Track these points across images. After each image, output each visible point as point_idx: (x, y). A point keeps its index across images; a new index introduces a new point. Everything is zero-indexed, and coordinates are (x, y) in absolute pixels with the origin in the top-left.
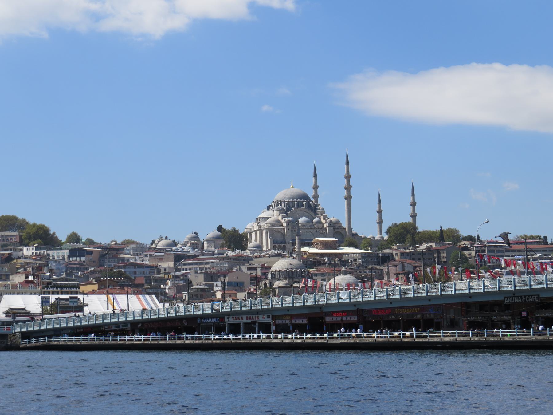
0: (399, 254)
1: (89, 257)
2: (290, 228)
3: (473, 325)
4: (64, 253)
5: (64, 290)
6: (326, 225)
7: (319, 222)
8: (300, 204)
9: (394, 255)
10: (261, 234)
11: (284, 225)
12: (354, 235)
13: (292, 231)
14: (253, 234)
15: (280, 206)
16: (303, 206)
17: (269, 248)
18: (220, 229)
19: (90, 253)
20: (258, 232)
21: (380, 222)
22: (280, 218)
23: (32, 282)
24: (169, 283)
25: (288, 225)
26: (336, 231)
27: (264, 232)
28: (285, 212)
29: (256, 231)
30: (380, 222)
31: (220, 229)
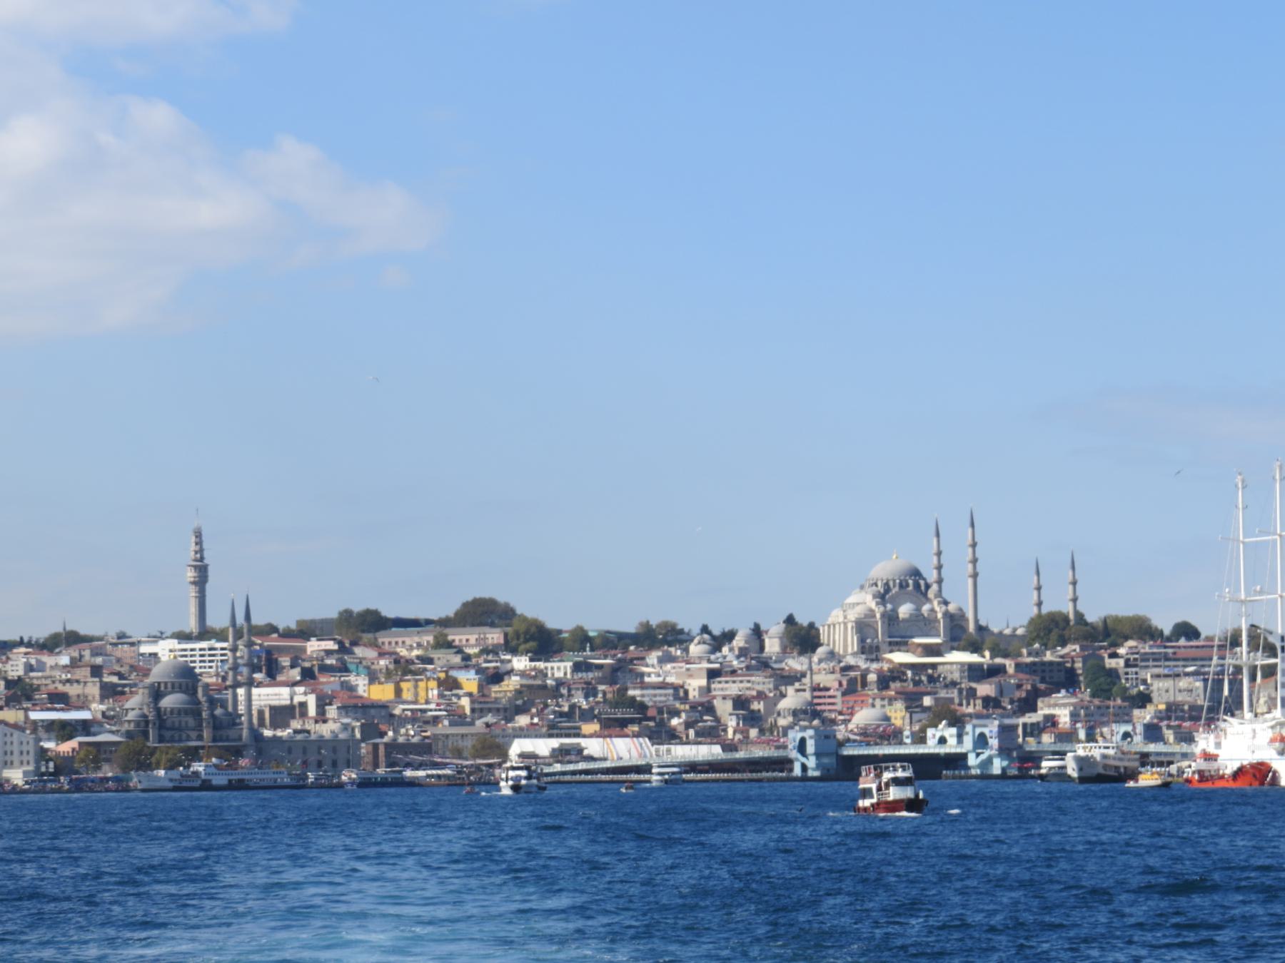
0: (1013, 665)
1: (598, 674)
2: (886, 620)
3: (751, 771)
4: (565, 668)
5: (567, 731)
6: (940, 616)
7: (932, 610)
8: (904, 584)
9: (1007, 666)
10: (846, 628)
11: (878, 616)
12: (981, 629)
13: (889, 625)
14: (837, 626)
15: (874, 588)
16: (908, 585)
17: (856, 649)
18: (790, 620)
19: (600, 667)
20: (842, 626)
21: (1039, 604)
22: (873, 605)
23: (537, 724)
24: (683, 715)
25: (883, 615)
26: (955, 623)
27: (849, 626)
28: (882, 598)
29: (839, 624)
30: (1039, 604)
31: (790, 620)
